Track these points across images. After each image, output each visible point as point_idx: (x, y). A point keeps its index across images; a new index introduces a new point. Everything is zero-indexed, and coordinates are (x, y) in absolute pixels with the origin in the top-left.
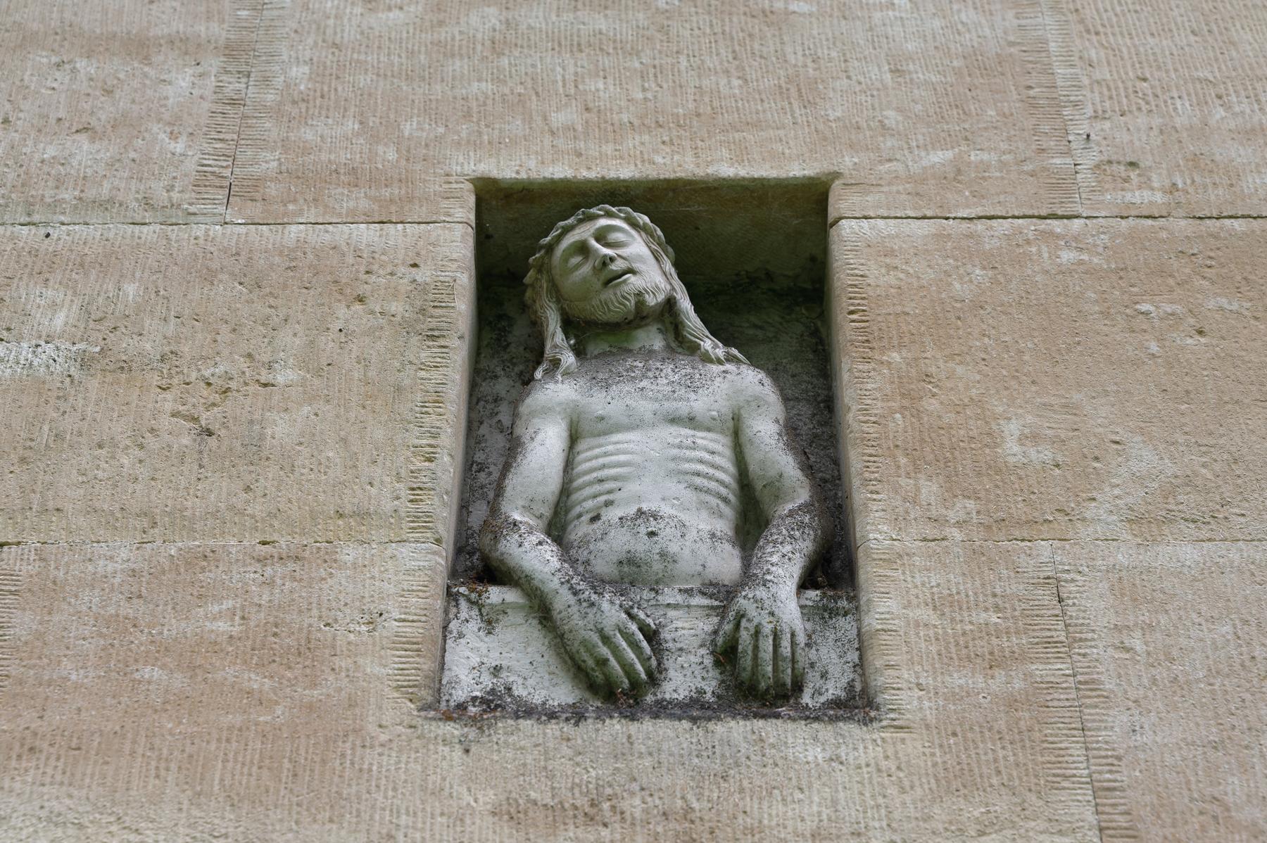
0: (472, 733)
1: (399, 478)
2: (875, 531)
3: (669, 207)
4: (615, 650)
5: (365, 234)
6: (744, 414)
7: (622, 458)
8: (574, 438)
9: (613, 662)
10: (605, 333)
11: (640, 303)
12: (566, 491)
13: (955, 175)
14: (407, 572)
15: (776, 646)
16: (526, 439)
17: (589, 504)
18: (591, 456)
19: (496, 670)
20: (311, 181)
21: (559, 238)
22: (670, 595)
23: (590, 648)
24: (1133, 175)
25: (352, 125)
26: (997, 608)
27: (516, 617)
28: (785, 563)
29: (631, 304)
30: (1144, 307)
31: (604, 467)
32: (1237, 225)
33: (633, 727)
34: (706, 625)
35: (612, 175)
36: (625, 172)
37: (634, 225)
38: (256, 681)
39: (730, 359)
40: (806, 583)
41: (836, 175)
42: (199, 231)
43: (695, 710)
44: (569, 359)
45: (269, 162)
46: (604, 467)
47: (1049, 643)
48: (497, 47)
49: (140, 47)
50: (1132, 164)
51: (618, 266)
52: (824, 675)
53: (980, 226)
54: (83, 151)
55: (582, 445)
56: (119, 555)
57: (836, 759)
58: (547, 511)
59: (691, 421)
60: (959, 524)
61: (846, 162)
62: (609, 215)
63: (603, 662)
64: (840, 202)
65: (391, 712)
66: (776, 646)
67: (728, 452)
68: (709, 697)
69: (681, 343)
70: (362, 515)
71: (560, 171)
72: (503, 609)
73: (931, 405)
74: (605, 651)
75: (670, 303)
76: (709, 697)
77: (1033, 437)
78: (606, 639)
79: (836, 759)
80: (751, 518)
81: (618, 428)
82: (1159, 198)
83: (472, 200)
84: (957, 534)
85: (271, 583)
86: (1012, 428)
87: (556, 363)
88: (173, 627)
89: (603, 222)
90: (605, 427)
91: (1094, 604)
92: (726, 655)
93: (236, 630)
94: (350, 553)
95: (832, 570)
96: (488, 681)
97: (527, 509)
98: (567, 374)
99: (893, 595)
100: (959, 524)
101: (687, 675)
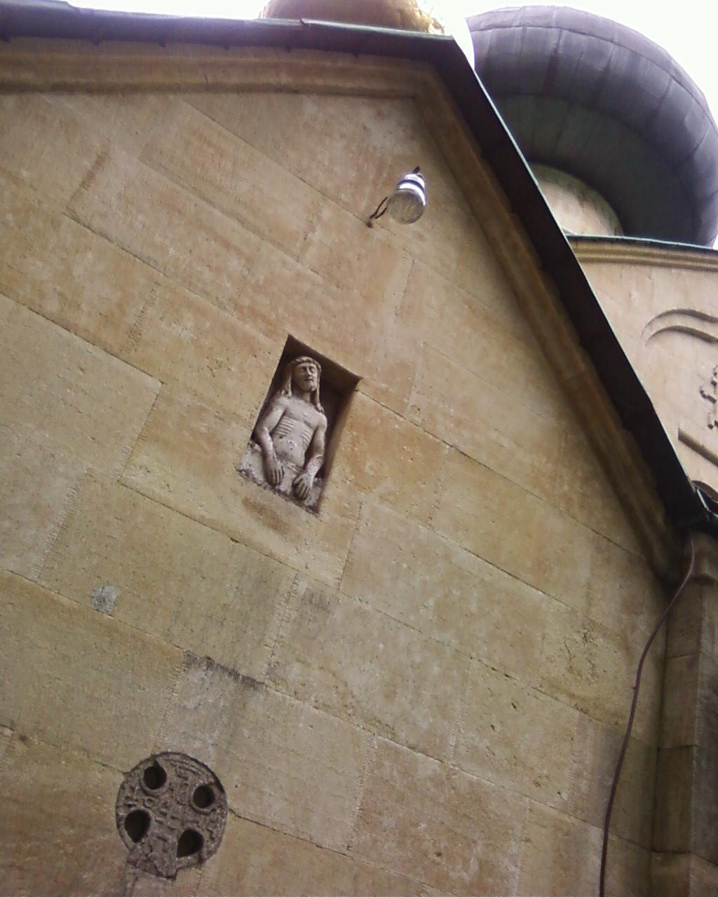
0: (244, 481)
1: (249, 411)
2: (335, 473)
3: (328, 367)
4: (276, 475)
5: (261, 338)
6: (320, 428)
7: (292, 426)
8: (284, 414)
9: (274, 478)
10: (299, 390)
11: (311, 389)
12: (277, 425)
13: (385, 392)
14: (244, 436)
15: (306, 489)
16: (274, 409)
17: (281, 433)
18: (286, 421)
19: (250, 465)
20: (254, 314)
21: (300, 363)
22: (290, 465)
23: (271, 471)
24: (418, 412)
25: (268, 303)
26: (349, 504)
27: (258, 454)
28: (314, 467)
29: (309, 388)
30: (405, 447)
31: (287, 426)
32: (431, 437)
33: (274, 496)
34: (294, 476)
35: (318, 351)
36: (321, 352)
37: (317, 366)
38: (206, 446)
39: (322, 412)
40: (317, 476)
41: (362, 378)
42: (226, 314)
43: (284, 494)
44: (290, 393)
45: (247, 302)
46: (287, 426)
47: (354, 516)
48: (307, 296)
49: (227, 245)
50: (419, 409)
51: (310, 378)
52: (310, 499)
53: (384, 408)
54: (207, 275)
55: (285, 417)
56: (187, 399)
57: (308, 522)
58: (271, 429)
59: (308, 424)
60: (350, 481)
61: (366, 377)
62: (314, 363)
63: (272, 476)
64: (360, 386)
65: (230, 469)
66: (306, 489)
67: (312, 434)
68: (288, 493)
69: (313, 402)
70: (239, 416)
71: (308, 344)
72: (256, 451)
73: (356, 449)
74: (274, 474)
75: (315, 391)
76: (288, 493)
77: (371, 468)
78: (276, 472)
79: (308, 522)
80: (309, 454)
81: (294, 419)
82: (420, 421)
83: (286, 340)
84: (348, 483)
85: (216, 423)
86: (368, 464)
87: (287, 393)
88: (193, 425)
89: (312, 365)
90: (291, 416)
91: (366, 512)
92: (295, 486)
93: (206, 432)
94: (234, 425)
95: (323, 474)
96: (248, 467)
97: (269, 428)
98: (289, 398)
99: (334, 489)
100: (350, 481)
101: (286, 486)
